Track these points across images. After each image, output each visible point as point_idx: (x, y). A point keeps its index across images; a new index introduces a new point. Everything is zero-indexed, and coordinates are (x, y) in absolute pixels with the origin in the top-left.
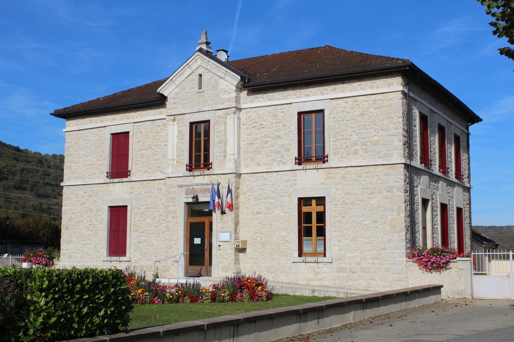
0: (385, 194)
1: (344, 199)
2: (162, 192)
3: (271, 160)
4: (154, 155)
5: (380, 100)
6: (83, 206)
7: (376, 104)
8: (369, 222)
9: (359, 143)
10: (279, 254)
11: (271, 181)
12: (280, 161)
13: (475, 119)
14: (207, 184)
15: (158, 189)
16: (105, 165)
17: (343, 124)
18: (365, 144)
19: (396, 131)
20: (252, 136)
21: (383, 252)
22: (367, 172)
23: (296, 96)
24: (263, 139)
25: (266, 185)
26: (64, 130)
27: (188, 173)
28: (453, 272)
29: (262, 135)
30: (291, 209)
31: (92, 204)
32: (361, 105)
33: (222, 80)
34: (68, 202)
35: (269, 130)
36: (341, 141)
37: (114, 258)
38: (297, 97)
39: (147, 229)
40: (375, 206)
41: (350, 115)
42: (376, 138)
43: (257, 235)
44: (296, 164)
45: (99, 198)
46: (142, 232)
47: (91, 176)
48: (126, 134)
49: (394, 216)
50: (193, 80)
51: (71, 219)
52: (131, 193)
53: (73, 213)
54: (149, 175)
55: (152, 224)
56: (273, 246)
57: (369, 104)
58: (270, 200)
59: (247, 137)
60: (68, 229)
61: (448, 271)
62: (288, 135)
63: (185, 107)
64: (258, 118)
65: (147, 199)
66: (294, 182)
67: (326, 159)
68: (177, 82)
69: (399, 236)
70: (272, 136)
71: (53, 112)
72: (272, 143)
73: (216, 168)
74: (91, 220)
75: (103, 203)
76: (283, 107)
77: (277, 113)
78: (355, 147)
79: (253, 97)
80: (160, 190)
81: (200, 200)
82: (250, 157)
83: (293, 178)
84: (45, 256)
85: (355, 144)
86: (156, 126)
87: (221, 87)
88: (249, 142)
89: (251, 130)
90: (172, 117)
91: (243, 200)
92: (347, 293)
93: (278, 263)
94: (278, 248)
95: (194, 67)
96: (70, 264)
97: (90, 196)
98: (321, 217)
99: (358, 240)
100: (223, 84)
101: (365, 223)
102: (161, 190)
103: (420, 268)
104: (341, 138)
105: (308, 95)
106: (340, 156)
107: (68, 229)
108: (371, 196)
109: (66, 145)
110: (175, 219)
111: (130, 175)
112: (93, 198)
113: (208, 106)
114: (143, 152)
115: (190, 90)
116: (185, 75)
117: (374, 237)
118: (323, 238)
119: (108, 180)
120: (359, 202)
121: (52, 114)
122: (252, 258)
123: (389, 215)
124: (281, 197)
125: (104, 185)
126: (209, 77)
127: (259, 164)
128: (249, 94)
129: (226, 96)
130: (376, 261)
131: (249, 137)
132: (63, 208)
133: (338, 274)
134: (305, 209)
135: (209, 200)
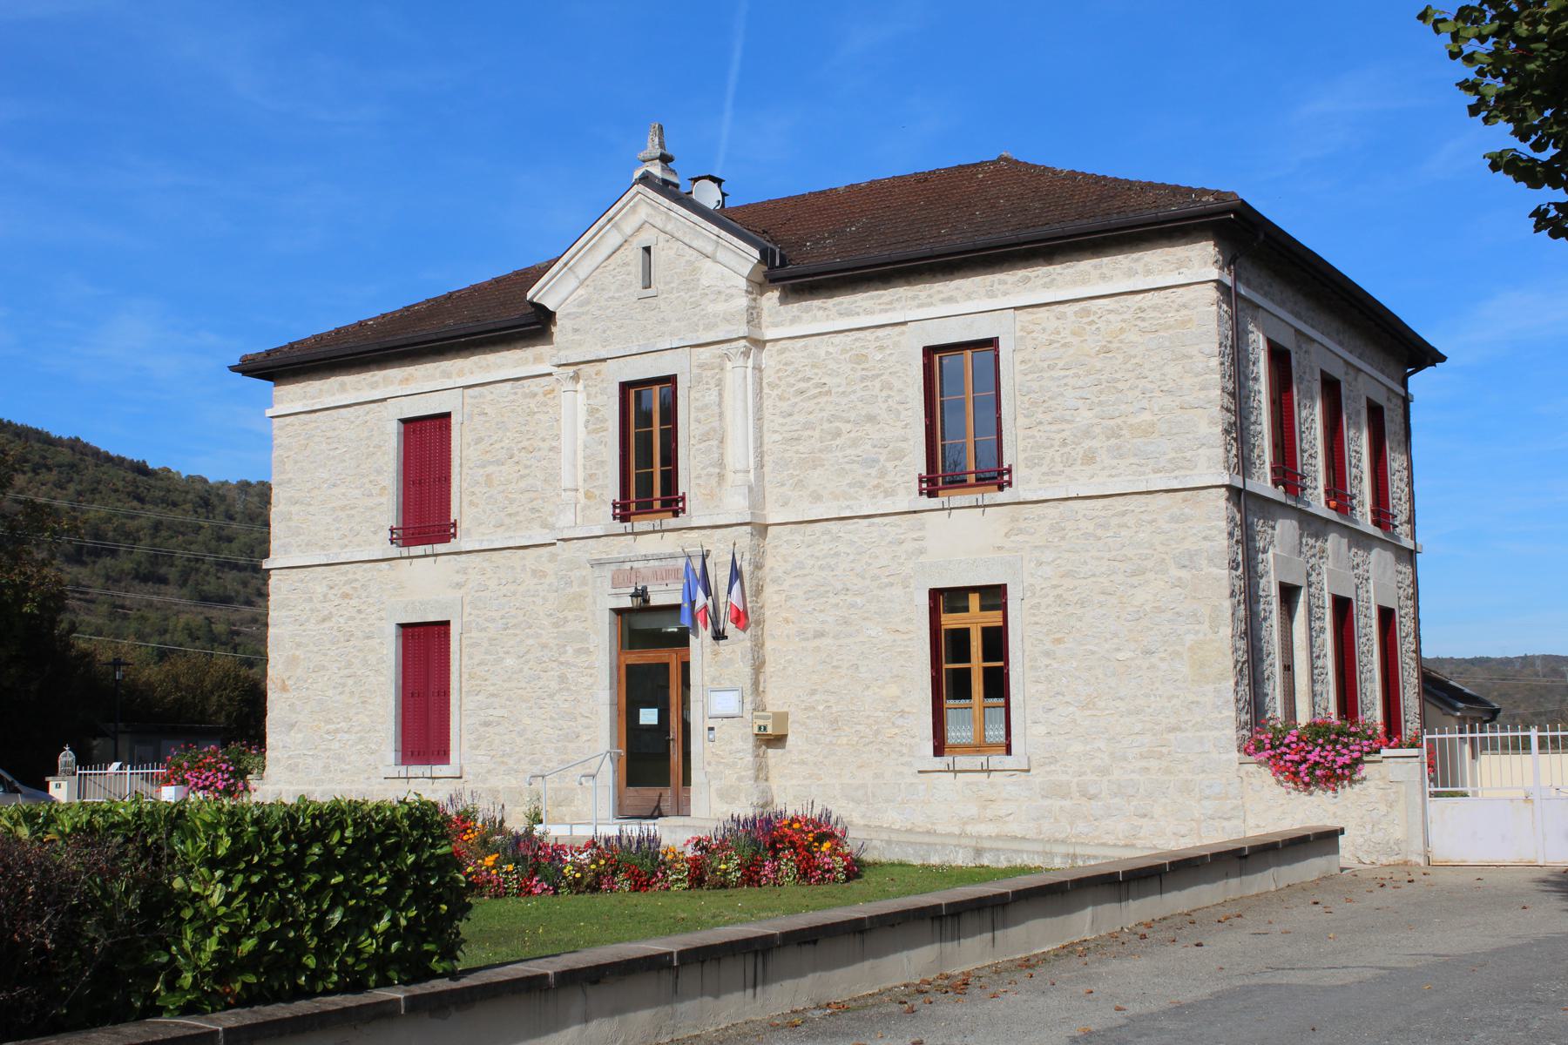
0: (1175, 572)
1: (1059, 591)
2: (547, 581)
3: (850, 485)
4: (522, 477)
5: (1155, 308)
6: (326, 625)
7: (1143, 320)
8: (1130, 654)
9: (1097, 430)
10: (880, 750)
11: (852, 543)
12: (877, 487)
13: (1423, 355)
14: (672, 557)
15: (534, 572)
16: (386, 508)
17: (1052, 378)
18: (1114, 433)
19: (1202, 395)
20: (795, 417)
21: (1171, 736)
22: (1124, 514)
23: (916, 302)
24: (826, 426)
25: (837, 554)
26: (269, 412)
27: (619, 527)
28: (1372, 790)
29: (825, 414)
30: (909, 620)
31: (352, 618)
32: (1101, 324)
33: (708, 262)
34: (284, 613)
35: (844, 401)
36: (1048, 428)
37: (416, 770)
38: (920, 306)
39: (506, 685)
41: (1071, 351)
42: (1146, 416)
43: (817, 697)
44: (921, 493)
45: (371, 601)
46: (493, 695)
47: (345, 541)
49: (1201, 636)
52: (459, 586)
53: (299, 645)
54: (507, 534)
55: (521, 671)
57: (1124, 321)
59: (781, 420)
60: (284, 689)
61: (1357, 787)
62: (899, 413)
63: (606, 340)
64: (813, 366)
66: (917, 545)
67: (1006, 478)
68: (583, 271)
69: (1217, 691)
70: (853, 415)
72: (852, 435)
73: (697, 509)
74: (349, 665)
75: (383, 614)
76: (880, 332)
77: (864, 352)
78: (1087, 444)
79: (795, 308)
80: (539, 574)
81: (652, 603)
82: (792, 476)
84: (224, 766)
85: (1087, 433)
86: (525, 396)
87: (705, 282)
88: (788, 436)
89: (793, 400)
90: (571, 370)
91: (776, 598)
92: (1074, 857)
93: (876, 776)
94: (877, 732)
95: (628, 228)
96: (292, 788)
97: (346, 596)
98: (996, 642)
99: (1102, 704)
100: (710, 274)
101: (1120, 656)
102: (545, 575)
103: (1278, 781)
104: (1048, 417)
105: (950, 299)
106: (1045, 469)
107: (284, 689)
108: (1135, 581)
109: (276, 453)
110: (584, 657)
111: (455, 535)
113: (671, 334)
114: (490, 469)
115: (618, 290)
116: (605, 251)
117: (1147, 696)
118: (1002, 701)
119: (394, 551)
120: (1102, 598)
121: (234, 369)
122: (803, 763)
123: (1189, 632)
124: (880, 588)
126: (672, 253)
127: (817, 498)
128: (784, 300)
129: (721, 307)
130: (1153, 764)
131: (788, 420)
132: (271, 631)
133: (1048, 802)
134: (950, 621)
135: (680, 601)
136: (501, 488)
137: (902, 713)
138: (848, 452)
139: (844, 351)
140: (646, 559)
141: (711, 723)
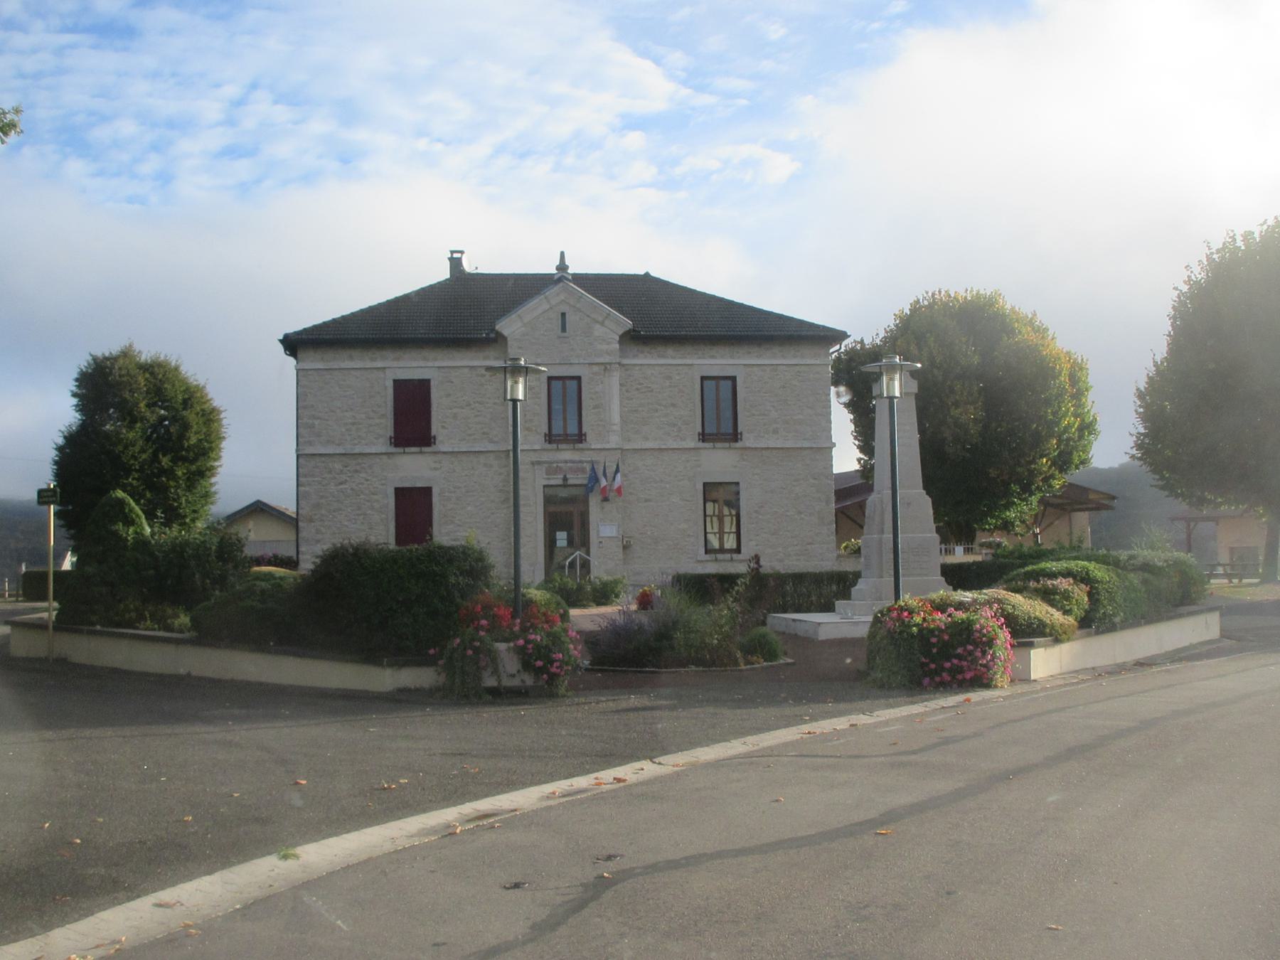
14: (581, 462)
16: (386, 426)
33: (598, 326)
48: (424, 385)
52: (436, 469)
53: (322, 497)
73: (593, 441)
74: (359, 509)
81: (570, 482)
87: (596, 334)
97: (356, 471)
100: (598, 330)
102: (491, 466)
105: (713, 357)
107: (311, 521)
112: (363, 475)
114: (455, 411)
119: (393, 450)
127: (647, 439)
129: (605, 347)
135: (585, 482)
140: (566, 462)
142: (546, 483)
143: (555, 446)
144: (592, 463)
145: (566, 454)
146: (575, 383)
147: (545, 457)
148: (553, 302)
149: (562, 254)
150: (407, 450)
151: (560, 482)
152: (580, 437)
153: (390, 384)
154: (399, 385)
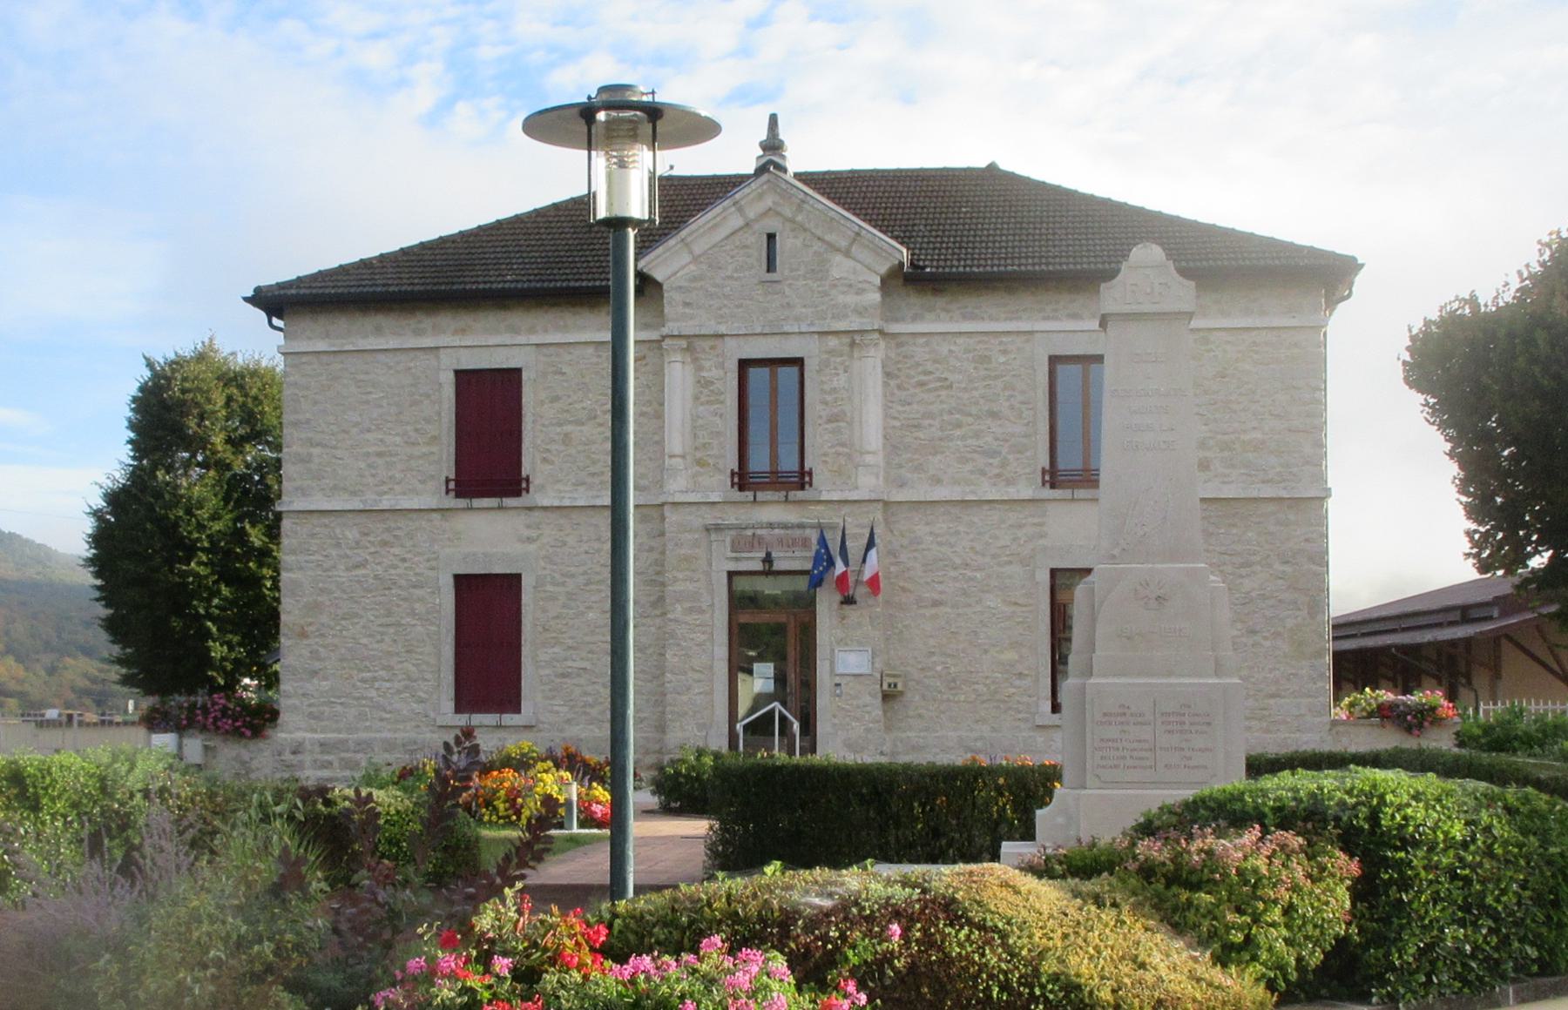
0: (1278, 566)
3: (972, 472)
7: (1257, 352)
12: (998, 475)
13: (914, 280)
14: (801, 526)
16: (442, 458)
20: (915, 406)
21: (1272, 701)
24: (946, 417)
27: (737, 495)
31: (395, 567)
33: (838, 258)
34: (302, 558)
35: (966, 396)
40: (1253, 594)
47: (385, 488)
48: (511, 378)
50: (746, 247)
51: (316, 607)
56: (979, 687)
58: (969, 573)
64: (935, 361)
65: (584, 556)
70: (974, 410)
71: (250, 293)
73: (825, 486)
74: (389, 614)
81: (777, 566)
82: (911, 460)
83: (1036, 520)
89: (912, 391)
94: (996, 692)
97: (385, 544)
100: (840, 267)
107: (303, 635)
108: (1243, 571)
112: (396, 550)
114: (569, 428)
115: (736, 270)
116: (723, 232)
119: (452, 502)
121: (246, 299)
124: (999, 565)
125: (435, 515)
126: (799, 242)
127: (937, 481)
129: (851, 299)
131: (907, 408)
135: (808, 566)
136: (581, 448)
137: (1020, 675)
138: (969, 442)
139: (967, 351)
140: (771, 526)
141: (837, 680)
142: (733, 567)
143: (749, 495)
144: (821, 528)
145: (772, 512)
146: (795, 370)
147: (731, 517)
148: (751, 215)
149: (773, 120)
150: (477, 502)
151: (758, 566)
152: (802, 479)
153: (448, 379)
154: (464, 378)
